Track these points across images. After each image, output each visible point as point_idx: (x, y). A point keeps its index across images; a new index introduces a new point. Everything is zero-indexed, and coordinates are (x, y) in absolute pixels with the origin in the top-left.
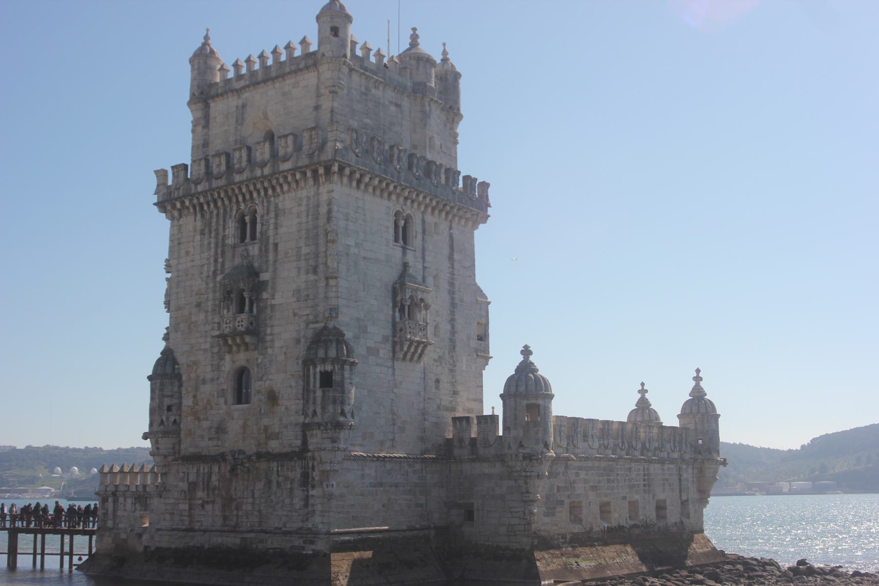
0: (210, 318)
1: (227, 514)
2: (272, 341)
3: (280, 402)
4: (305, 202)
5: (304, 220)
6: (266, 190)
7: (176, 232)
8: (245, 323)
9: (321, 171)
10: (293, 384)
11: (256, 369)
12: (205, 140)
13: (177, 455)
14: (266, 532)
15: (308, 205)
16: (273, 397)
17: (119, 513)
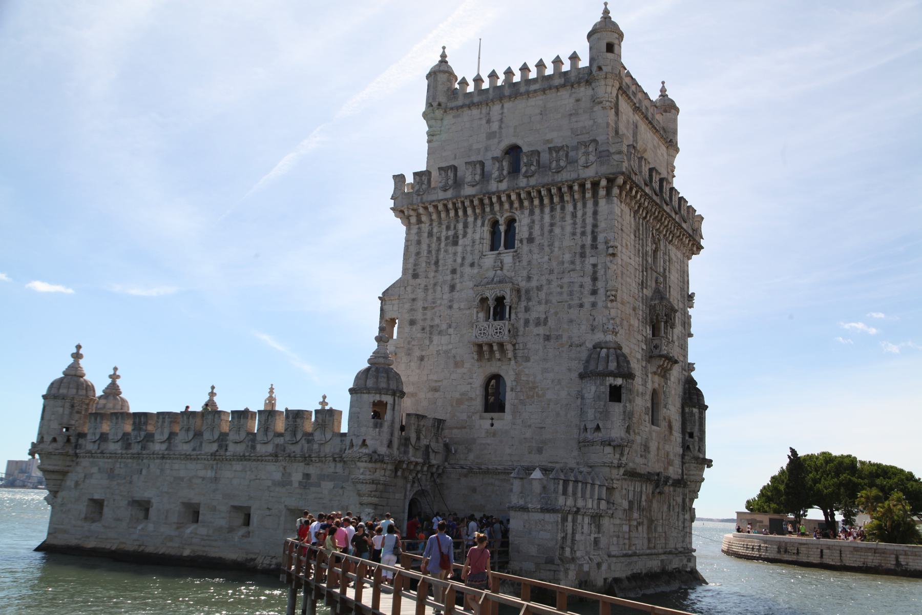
3: (674, 432)
14: (670, 553)
16: (670, 427)
17: (578, 537)
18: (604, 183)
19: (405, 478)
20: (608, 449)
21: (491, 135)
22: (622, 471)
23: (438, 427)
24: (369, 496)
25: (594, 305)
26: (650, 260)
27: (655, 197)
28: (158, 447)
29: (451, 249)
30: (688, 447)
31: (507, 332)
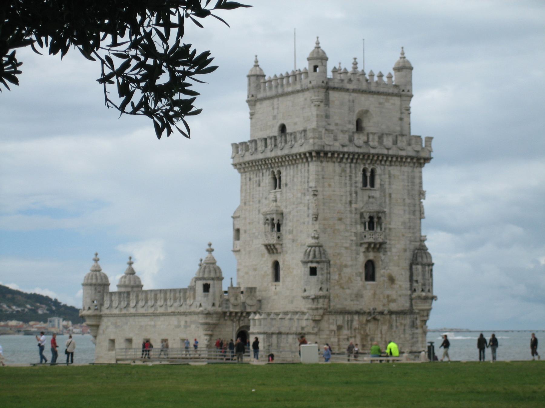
0: (349, 228)
1: (365, 343)
2: (390, 248)
3: (396, 282)
4: (406, 174)
5: (406, 184)
6: (386, 161)
7: (320, 169)
8: (382, 237)
9: (422, 161)
10: (403, 273)
11: (380, 263)
12: (327, 114)
13: (328, 310)
15: (408, 176)
16: (392, 280)
17: (282, 345)
18: (308, 155)
19: (232, 320)
20: (310, 301)
21: (275, 117)
22: (321, 312)
23: (251, 292)
24: (206, 330)
25: (308, 222)
26: (360, 185)
27: (357, 150)
28: (132, 311)
29: (258, 188)
30: (415, 290)
31: (275, 238)
